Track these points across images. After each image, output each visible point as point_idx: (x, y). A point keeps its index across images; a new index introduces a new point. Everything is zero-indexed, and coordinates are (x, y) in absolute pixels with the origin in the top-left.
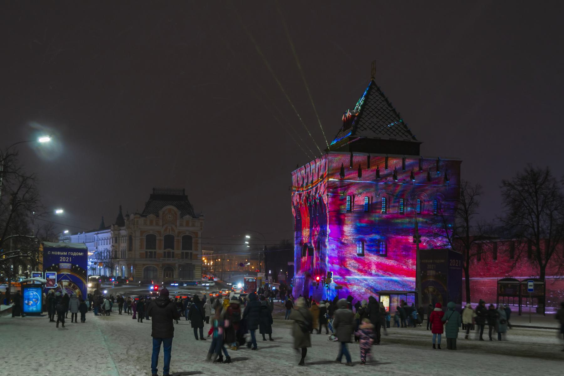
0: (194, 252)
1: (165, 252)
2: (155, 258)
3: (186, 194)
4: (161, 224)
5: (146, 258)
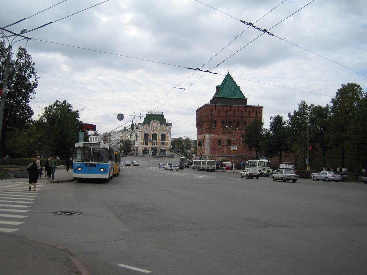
4: (151, 128)
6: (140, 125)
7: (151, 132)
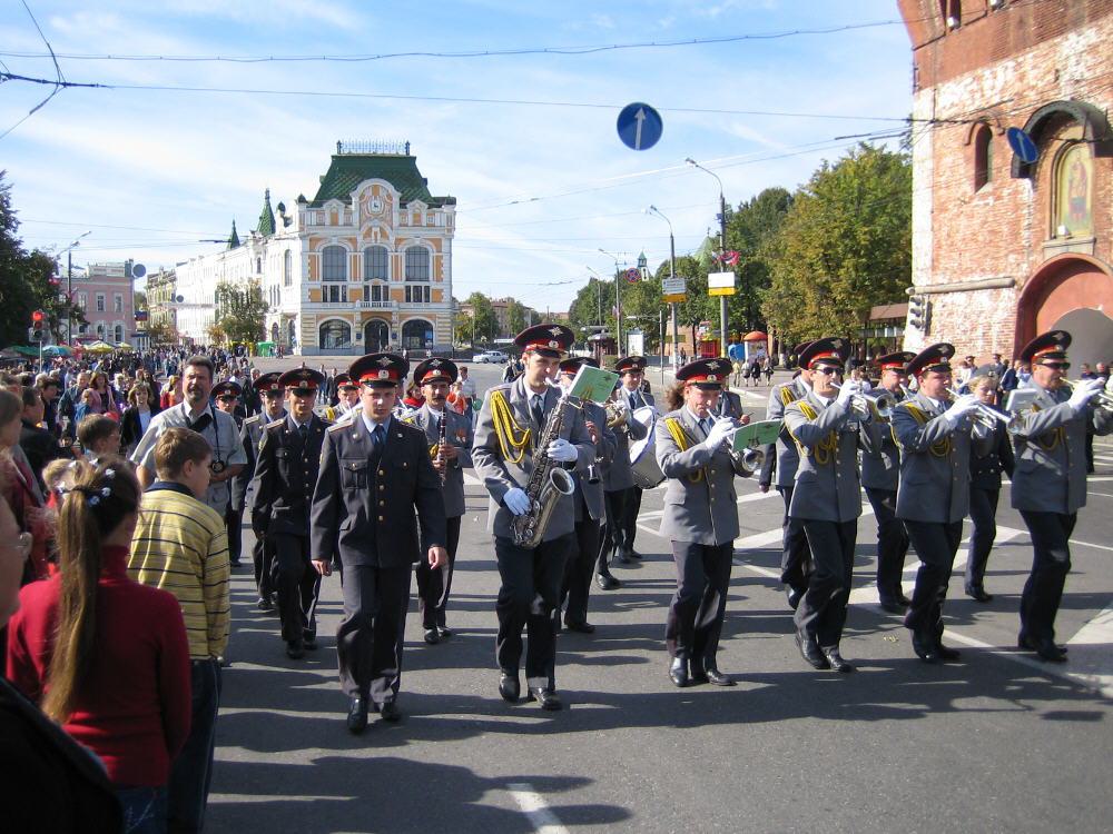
0: (433, 285)
1: (367, 288)
2: (344, 300)
3: (411, 154)
4: (355, 219)
5: (325, 300)
6: (304, 206)
7: (360, 239)
